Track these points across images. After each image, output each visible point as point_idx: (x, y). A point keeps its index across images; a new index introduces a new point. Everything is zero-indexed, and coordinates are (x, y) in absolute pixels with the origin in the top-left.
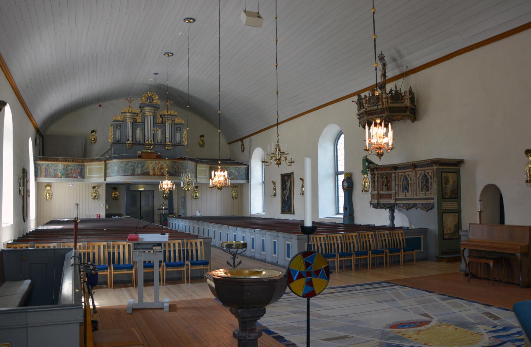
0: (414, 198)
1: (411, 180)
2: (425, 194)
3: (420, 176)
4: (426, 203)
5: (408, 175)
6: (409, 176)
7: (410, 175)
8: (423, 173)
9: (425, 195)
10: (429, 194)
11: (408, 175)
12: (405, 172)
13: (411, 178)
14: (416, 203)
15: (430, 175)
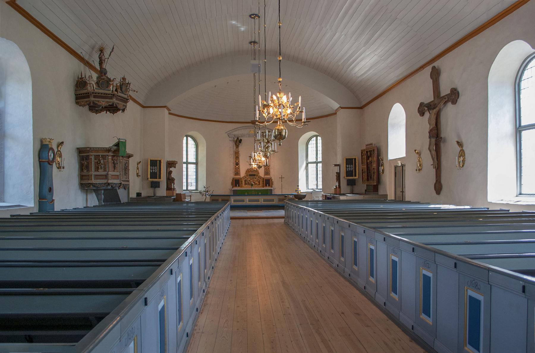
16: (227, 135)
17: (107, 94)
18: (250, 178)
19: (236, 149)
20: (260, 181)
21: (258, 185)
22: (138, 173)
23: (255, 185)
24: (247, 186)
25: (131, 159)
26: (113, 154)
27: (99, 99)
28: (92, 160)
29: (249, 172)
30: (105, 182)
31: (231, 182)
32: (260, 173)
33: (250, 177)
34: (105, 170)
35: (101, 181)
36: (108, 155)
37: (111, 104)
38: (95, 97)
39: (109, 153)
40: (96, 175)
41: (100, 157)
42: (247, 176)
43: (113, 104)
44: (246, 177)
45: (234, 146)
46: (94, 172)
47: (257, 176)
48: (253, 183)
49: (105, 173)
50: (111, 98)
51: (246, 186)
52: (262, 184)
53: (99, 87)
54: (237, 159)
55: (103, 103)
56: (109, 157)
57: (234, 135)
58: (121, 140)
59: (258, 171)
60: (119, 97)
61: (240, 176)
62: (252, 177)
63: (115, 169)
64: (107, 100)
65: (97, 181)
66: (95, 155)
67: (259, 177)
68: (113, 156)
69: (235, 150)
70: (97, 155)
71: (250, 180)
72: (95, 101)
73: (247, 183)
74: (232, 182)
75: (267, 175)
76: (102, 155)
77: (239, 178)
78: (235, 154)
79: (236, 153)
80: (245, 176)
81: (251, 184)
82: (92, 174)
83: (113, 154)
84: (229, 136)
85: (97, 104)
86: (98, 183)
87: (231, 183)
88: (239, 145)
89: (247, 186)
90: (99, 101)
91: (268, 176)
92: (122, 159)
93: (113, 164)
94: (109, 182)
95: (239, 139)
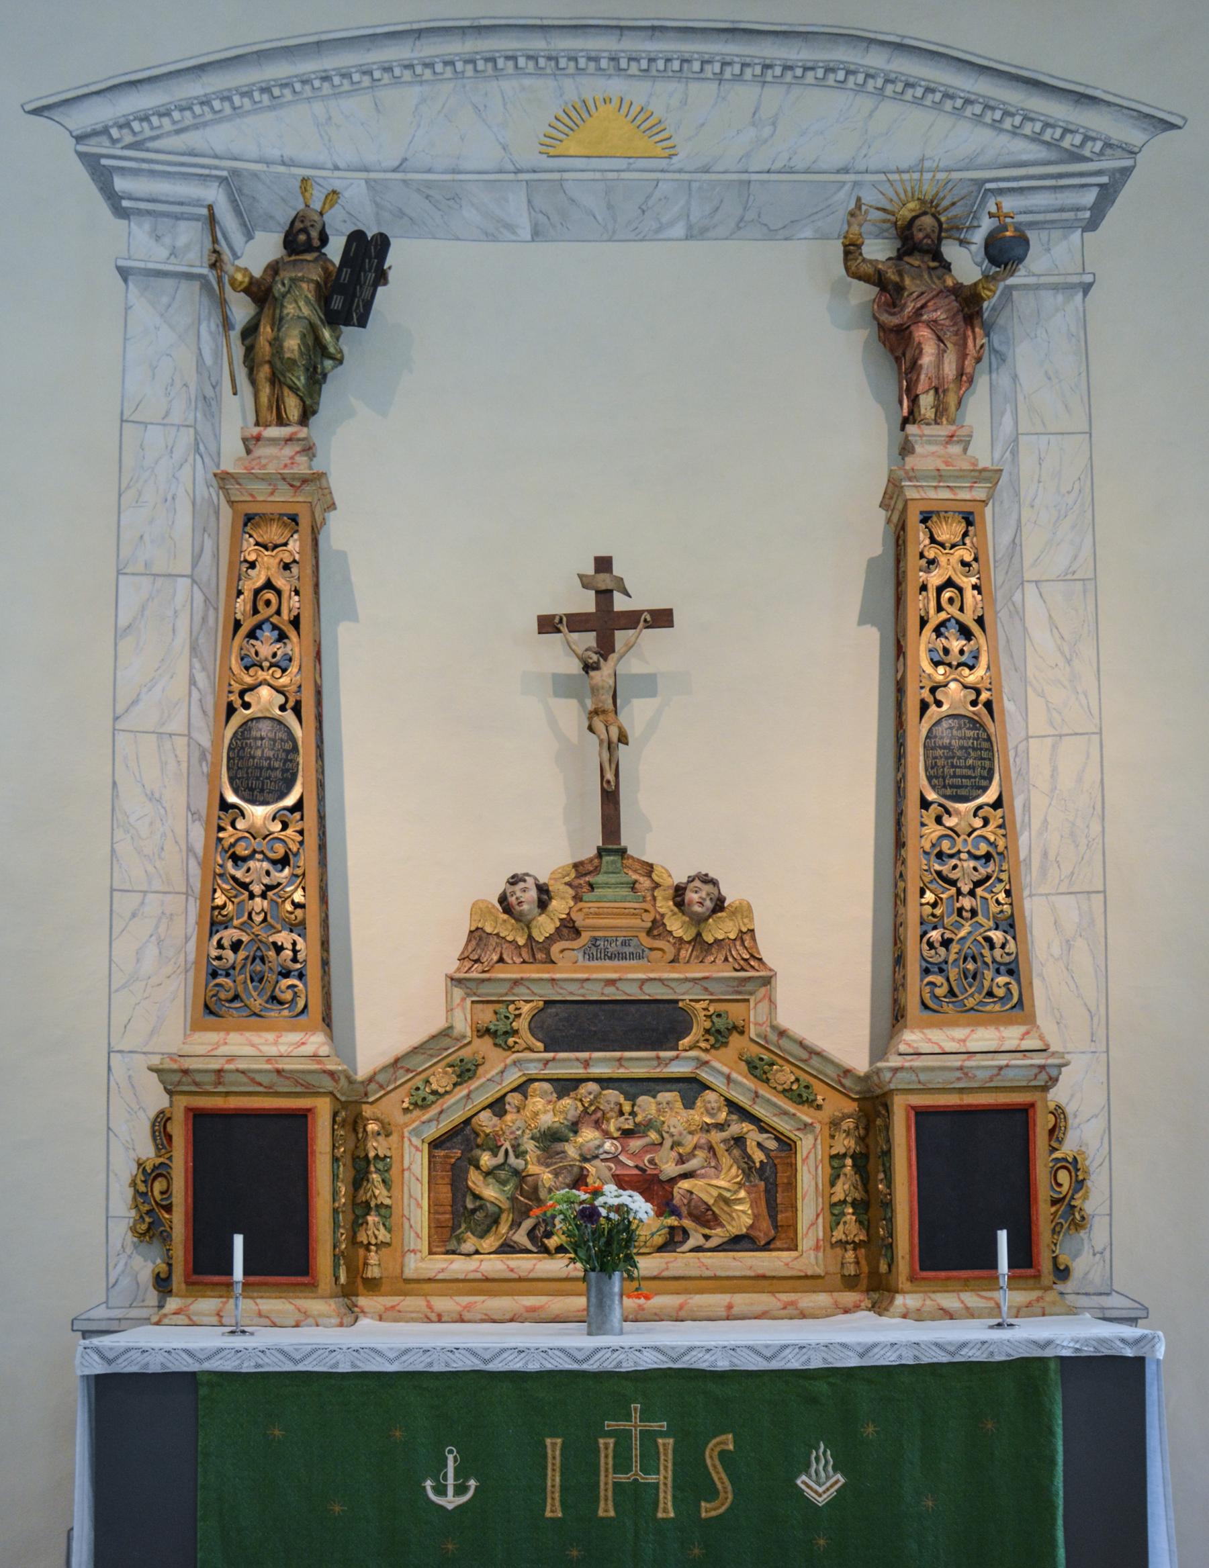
16: (81, 173)
18: (565, 1086)
19: (250, 443)
20: (787, 1145)
21: (737, 1243)
23: (672, 1241)
24: (495, 1265)
29: (538, 951)
31: (125, 1170)
32: (782, 990)
33: (568, 1064)
42: (500, 1036)
44: (465, 1072)
45: (208, 404)
47: (719, 1036)
48: (640, 1207)
51: (459, 1266)
52: (835, 1211)
54: (266, 647)
57: (232, 183)
59: (747, 935)
61: (316, 1042)
62: (603, 1063)
67: (758, 1069)
69: (231, 455)
71: (551, 1139)
73: (491, 1192)
74: (152, 1174)
75: (973, 1015)
77: (303, 1084)
78: (236, 547)
79: (249, 519)
80: (446, 1033)
81: (589, 1214)
84: (102, 175)
87: (140, 1196)
88: (316, 379)
89: (495, 1265)
91: (984, 1037)
95: (335, 250)
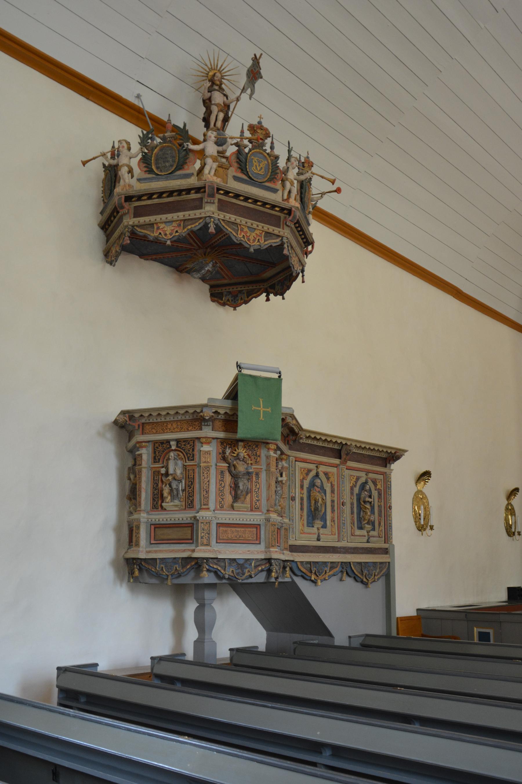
0: (340, 548)
1: (333, 492)
2: (369, 538)
3: (355, 486)
4: (375, 563)
5: (326, 474)
6: (328, 479)
7: (330, 475)
8: (363, 480)
9: (368, 542)
10: (375, 539)
11: (326, 474)
12: (318, 464)
13: (332, 486)
14: (350, 563)
15: (378, 488)
17: (180, 192)
22: (511, 527)
25: (395, 466)
26: (221, 435)
27: (152, 219)
28: (144, 464)
30: (185, 555)
34: (190, 505)
35: (172, 551)
36: (199, 439)
37: (196, 226)
38: (138, 213)
39: (201, 429)
40: (157, 527)
41: (173, 448)
43: (206, 226)
46: (148, 513)
49: (185, 516)
50: (198, 205)
53: (151, 171)
55: (168, 229)
56: (206, 448)
58: (244, 372)
60: (234, 201)
63: (236, 498)
64: (181, 215)
65: (156, 552)
66: (155, 442)
68: (224, 443)
70: (162, 442)
72: (141, 226)
76: (178, 441)
82: (138, 520)
83: (221, 435)
85: (145, 236)
86: (162, 560)
90: (151, 225)
92: (336, 466)
93: (228, 478)
94: (195, 555)
